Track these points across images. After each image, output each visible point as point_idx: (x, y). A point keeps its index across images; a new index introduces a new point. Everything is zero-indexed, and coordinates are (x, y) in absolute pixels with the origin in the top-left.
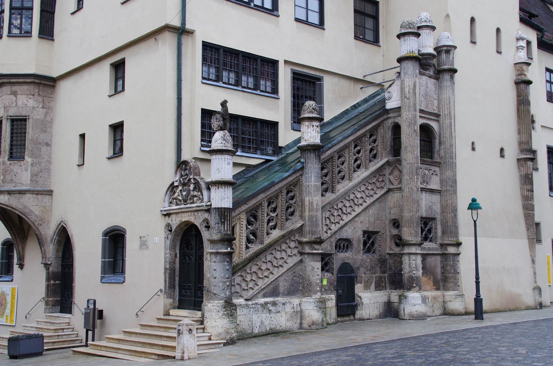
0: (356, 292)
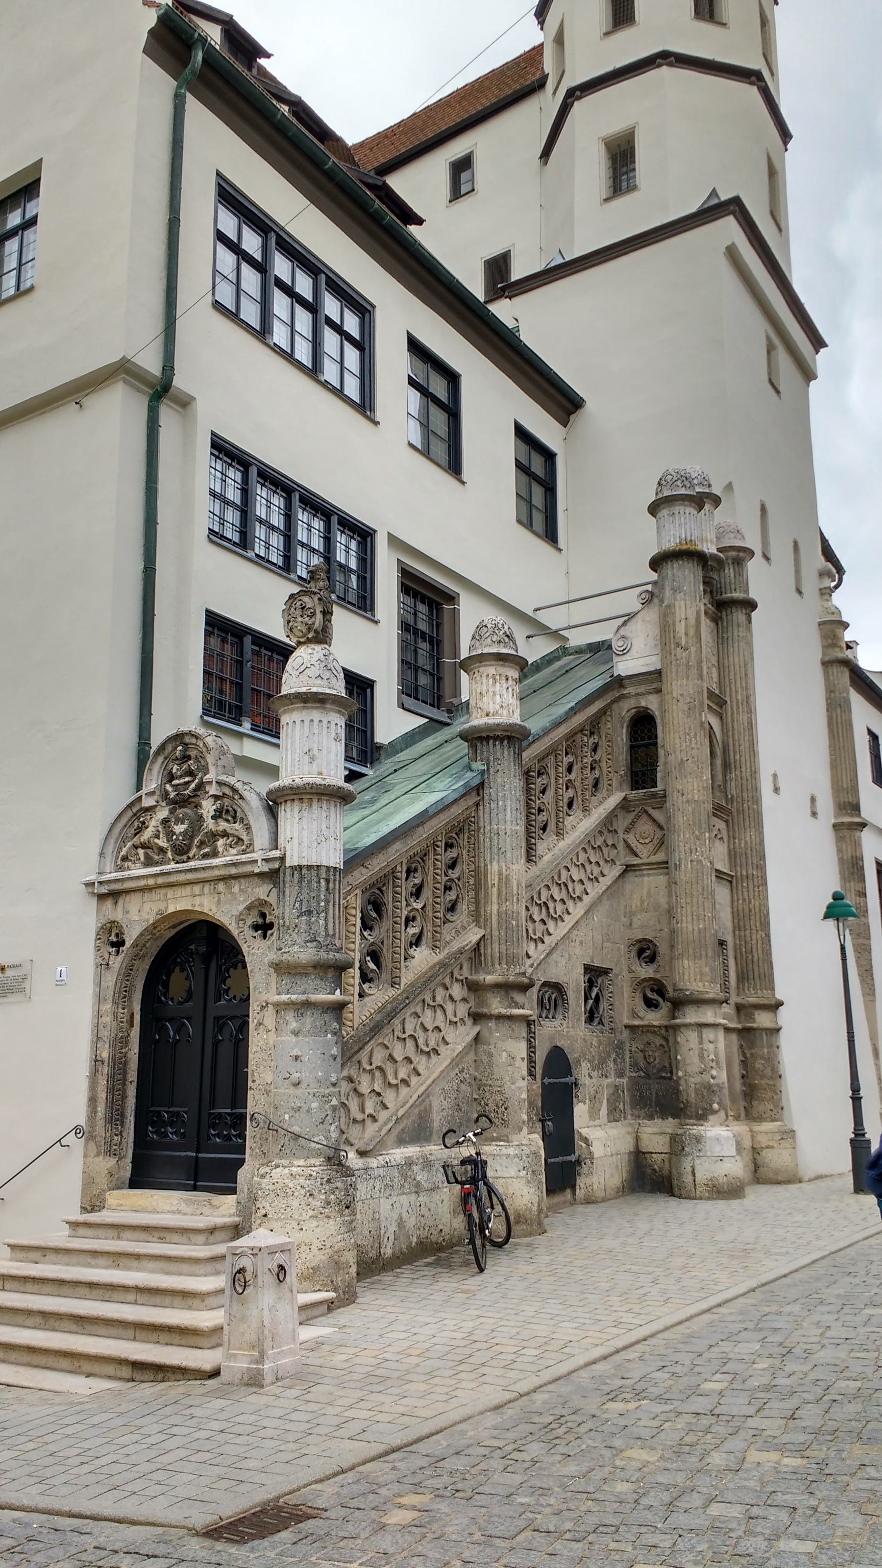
0: (576, 1126)
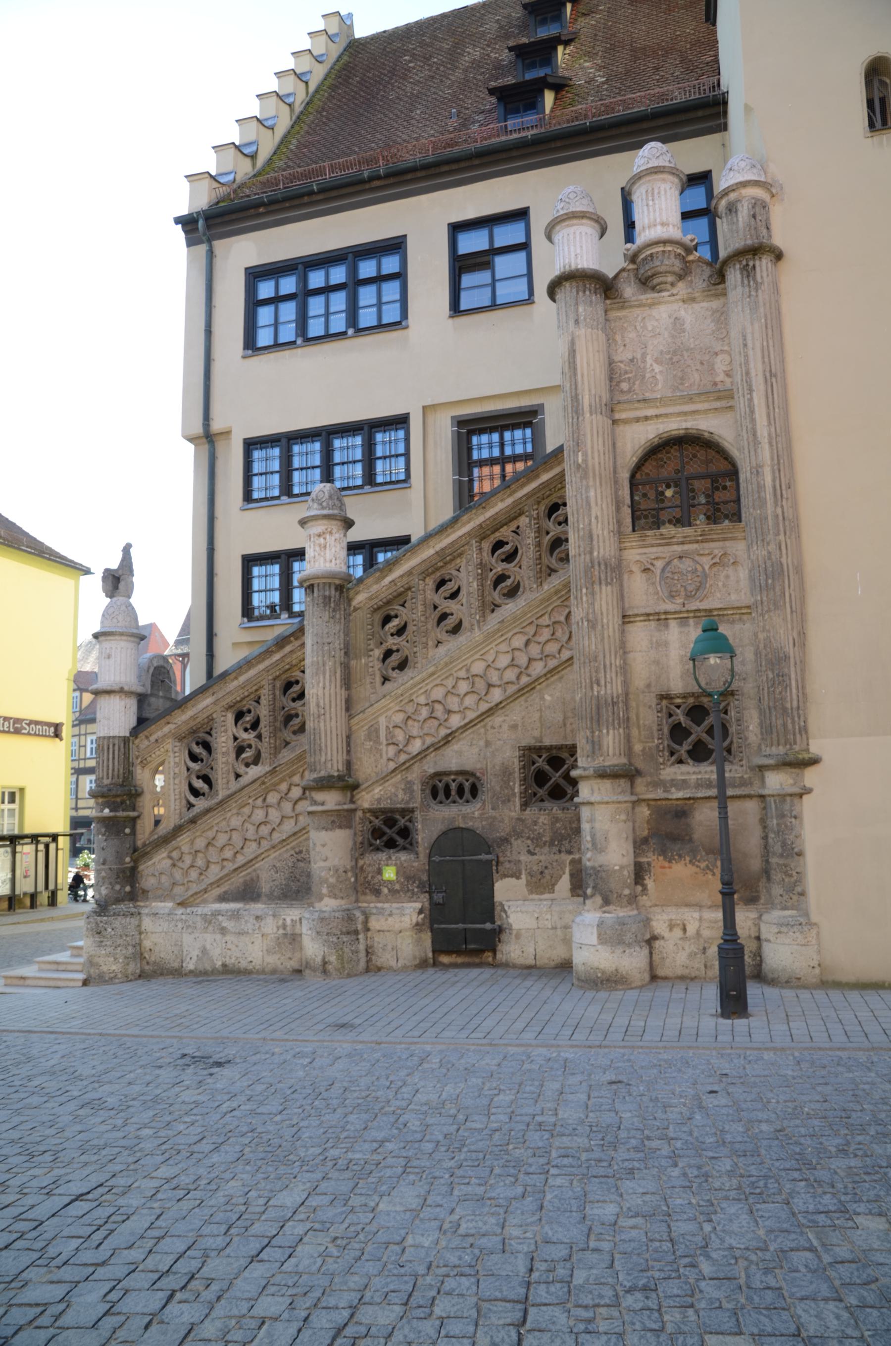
0: (496, 899)
